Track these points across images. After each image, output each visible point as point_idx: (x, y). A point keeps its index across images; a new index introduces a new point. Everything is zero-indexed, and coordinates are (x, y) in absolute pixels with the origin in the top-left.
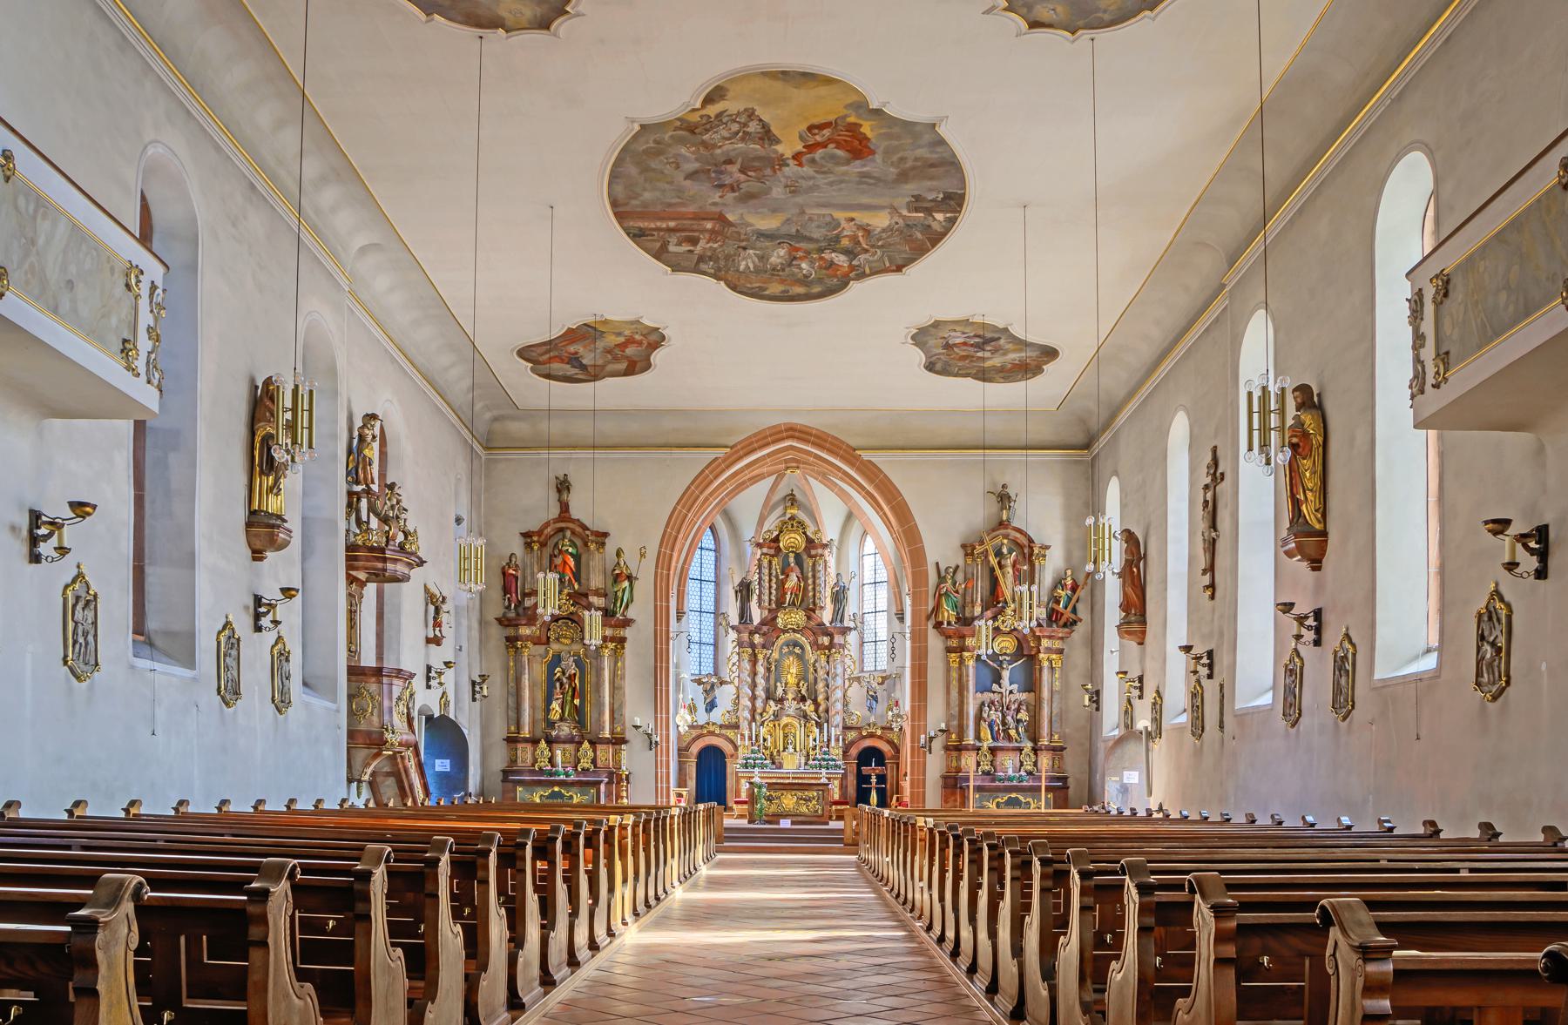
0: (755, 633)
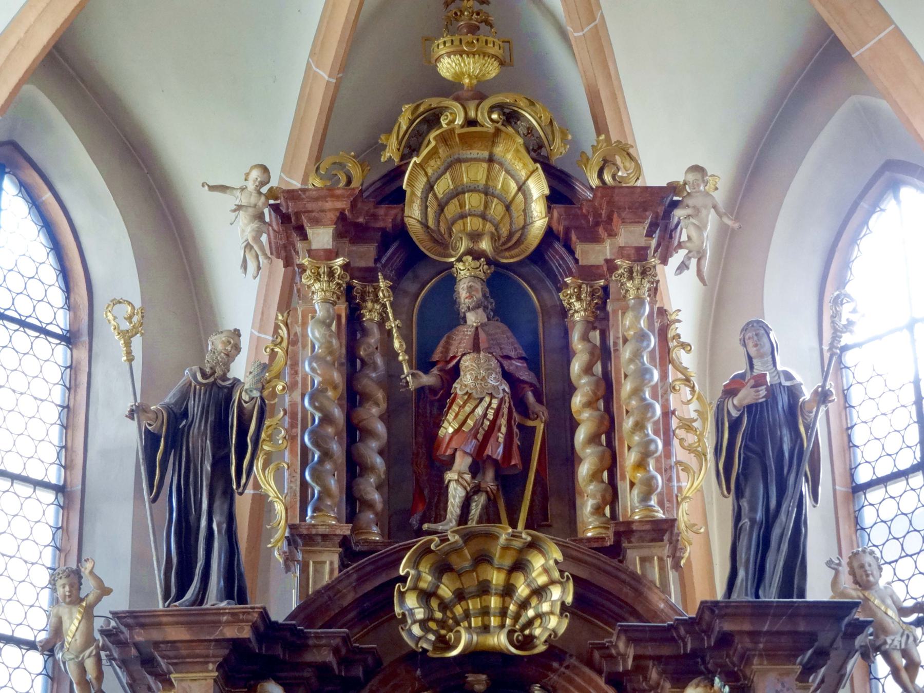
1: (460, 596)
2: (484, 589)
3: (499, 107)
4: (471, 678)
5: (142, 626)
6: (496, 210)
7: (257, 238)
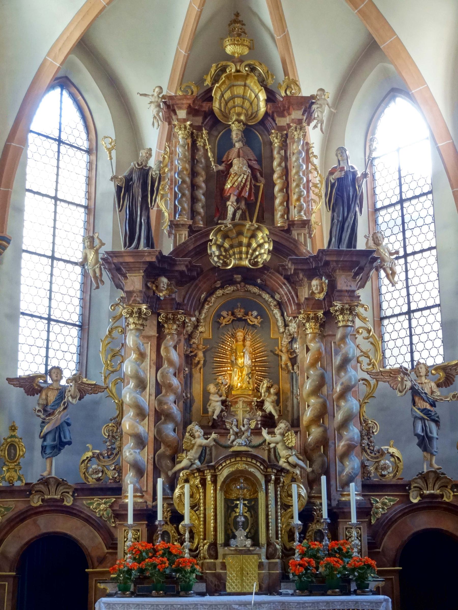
0: (160, 275)
1: (232, 247)
2: (240, 244)
3: (249, 65)
4: (235, 276)
5: (116, 256)
6: (247, 104)
7: (158, 114)
